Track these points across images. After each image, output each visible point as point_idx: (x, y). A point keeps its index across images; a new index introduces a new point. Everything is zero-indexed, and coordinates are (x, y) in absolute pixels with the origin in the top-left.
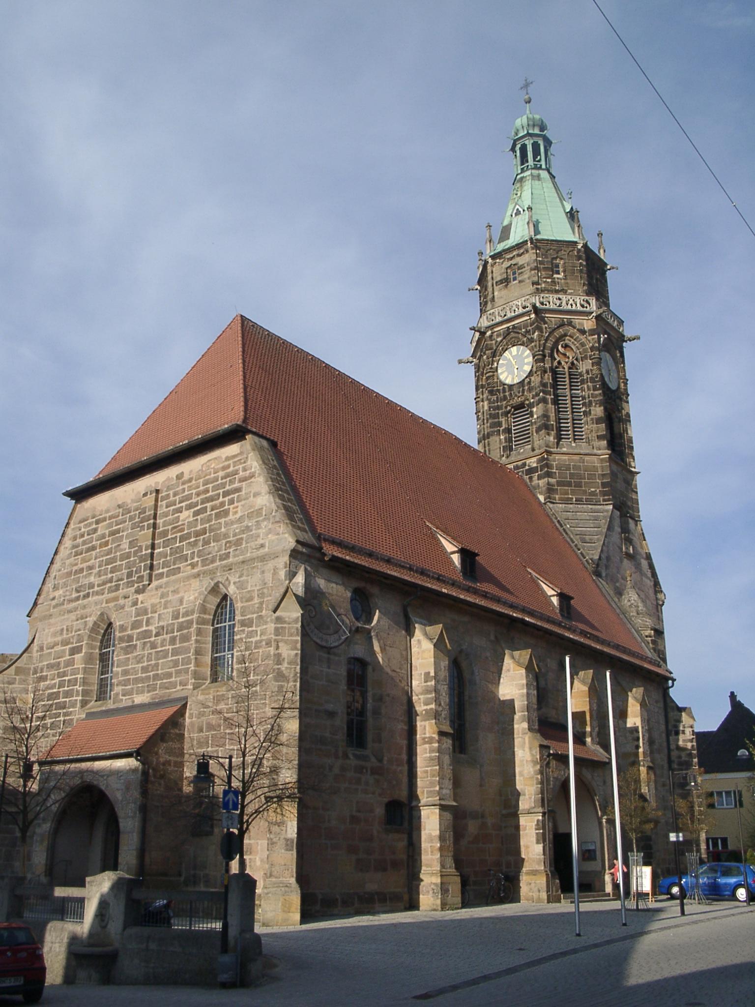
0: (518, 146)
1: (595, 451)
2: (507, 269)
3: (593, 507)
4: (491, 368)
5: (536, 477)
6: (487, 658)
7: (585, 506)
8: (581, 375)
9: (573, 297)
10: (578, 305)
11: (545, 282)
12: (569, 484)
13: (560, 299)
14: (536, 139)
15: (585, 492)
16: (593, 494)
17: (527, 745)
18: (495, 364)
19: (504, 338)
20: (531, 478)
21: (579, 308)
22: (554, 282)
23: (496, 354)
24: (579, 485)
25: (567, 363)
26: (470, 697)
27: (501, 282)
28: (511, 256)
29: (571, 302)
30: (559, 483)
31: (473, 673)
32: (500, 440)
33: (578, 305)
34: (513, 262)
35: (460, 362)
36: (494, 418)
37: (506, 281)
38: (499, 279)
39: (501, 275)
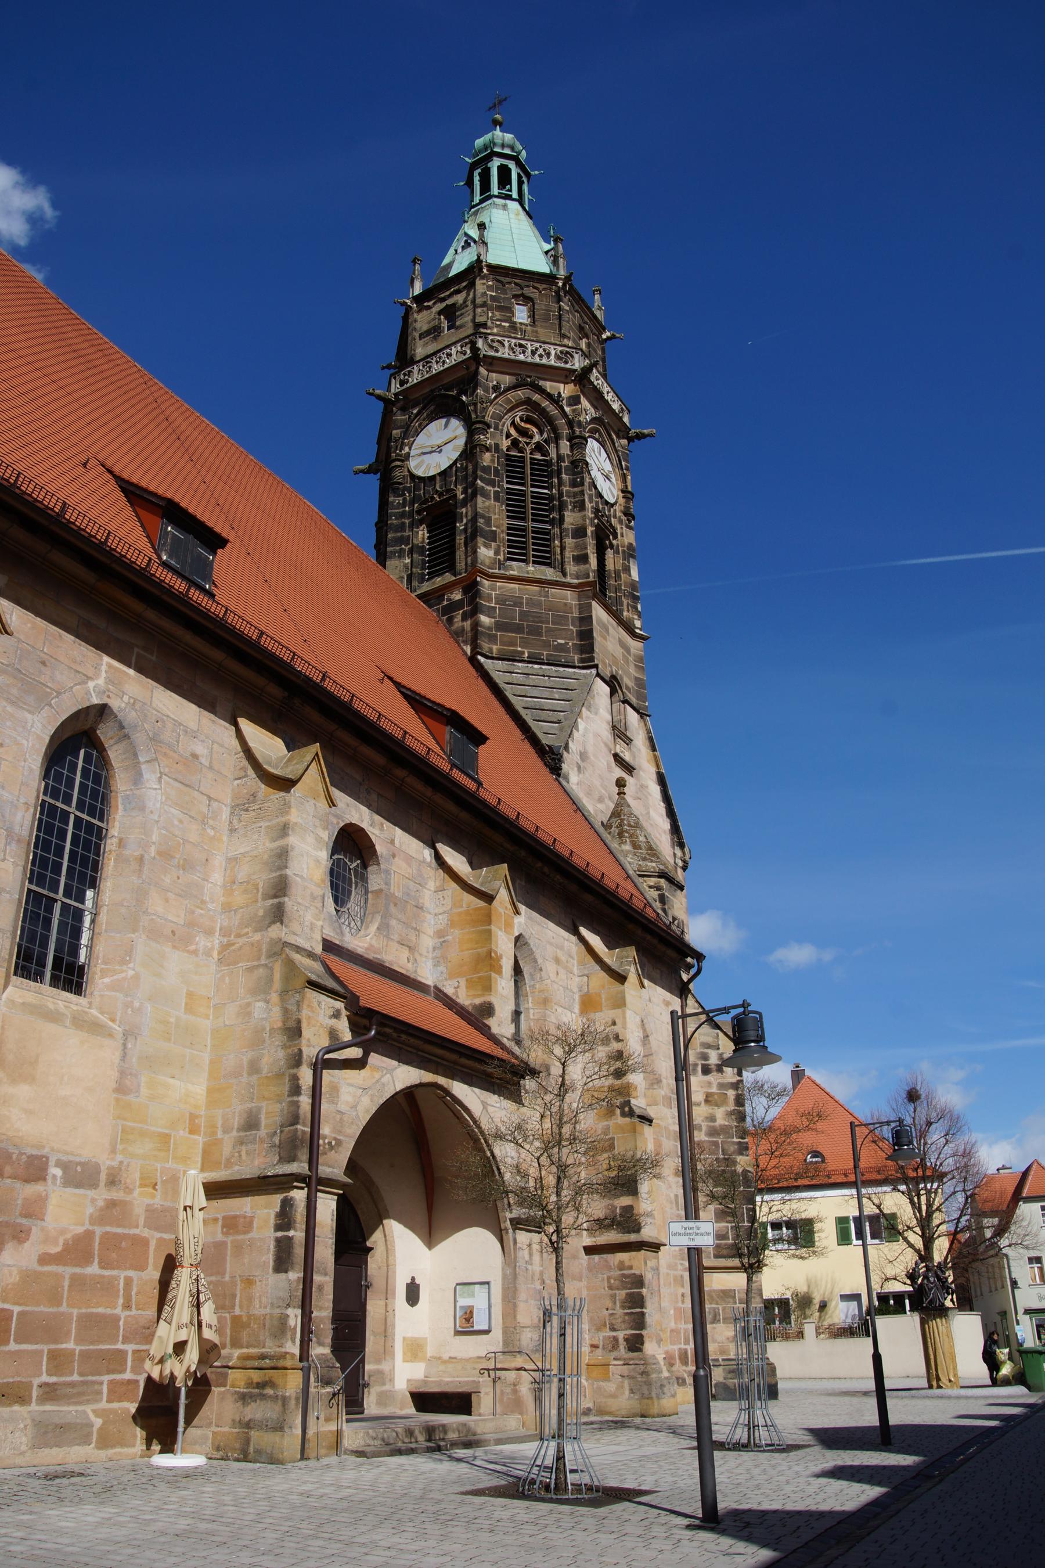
0: (476, 173)
1: (569, 580)
2: (440, 313)
3: (562, 669)
4: (401, 455)
5: (459, 617)
6: (195, 756)
7: (544, 667)
8: (549, 463)
9: (546, 346)
10: (552, 357)
11: (498, 326)
12: (518, 629)
13: (521, 346)
14: (505, 162)
15: (546, 645)
16: (562, 648)
17: (277, 984)
18: (407, 449)
19: (423, 408)
20: (450, 621)
21: (552, 362)
22: (514, 327)
23: (410, 432)
24: (536, 631)
25: (528, 444)
26: (121, 843)
27: (428, 333)
28: (448, 293)
29: (540, 351)
30: (500, 626)
31: (137, 779)
32: (405, 565)
33: (552, 357)
34: (449, 302)
35: (356, 473)
36: (396, 531)
37: (434, 332)
38: (425, 328)
39: (429, 322)
